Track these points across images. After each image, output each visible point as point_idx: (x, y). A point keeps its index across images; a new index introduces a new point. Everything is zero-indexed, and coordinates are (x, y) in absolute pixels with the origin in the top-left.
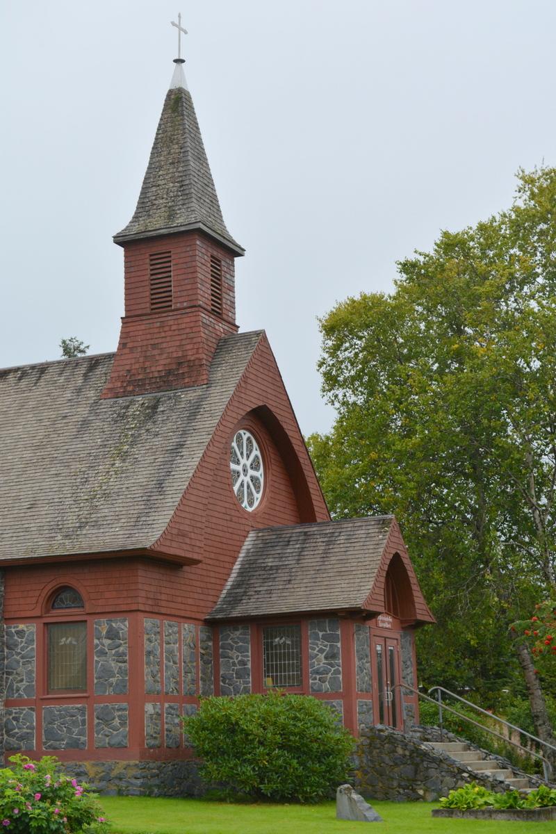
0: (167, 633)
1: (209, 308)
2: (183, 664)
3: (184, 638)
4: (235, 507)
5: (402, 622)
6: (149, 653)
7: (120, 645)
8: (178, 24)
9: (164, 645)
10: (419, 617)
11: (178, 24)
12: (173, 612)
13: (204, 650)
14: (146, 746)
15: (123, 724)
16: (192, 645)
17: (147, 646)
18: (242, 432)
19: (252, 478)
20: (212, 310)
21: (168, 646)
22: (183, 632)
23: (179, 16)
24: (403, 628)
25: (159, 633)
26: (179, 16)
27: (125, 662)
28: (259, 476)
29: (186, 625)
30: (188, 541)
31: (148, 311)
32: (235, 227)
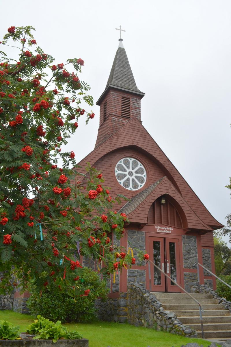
1: (120, 116)
4: (118, 188)
5: (184, 230)
8: (119, 28)
10: (189, 227)
11: (119, 28)
18: (128, 158)
20: (122, 116)
23: (120, 26)
24: (186, 234)
26: (120, 26)
28: (144, 177)
32: (140, 86)
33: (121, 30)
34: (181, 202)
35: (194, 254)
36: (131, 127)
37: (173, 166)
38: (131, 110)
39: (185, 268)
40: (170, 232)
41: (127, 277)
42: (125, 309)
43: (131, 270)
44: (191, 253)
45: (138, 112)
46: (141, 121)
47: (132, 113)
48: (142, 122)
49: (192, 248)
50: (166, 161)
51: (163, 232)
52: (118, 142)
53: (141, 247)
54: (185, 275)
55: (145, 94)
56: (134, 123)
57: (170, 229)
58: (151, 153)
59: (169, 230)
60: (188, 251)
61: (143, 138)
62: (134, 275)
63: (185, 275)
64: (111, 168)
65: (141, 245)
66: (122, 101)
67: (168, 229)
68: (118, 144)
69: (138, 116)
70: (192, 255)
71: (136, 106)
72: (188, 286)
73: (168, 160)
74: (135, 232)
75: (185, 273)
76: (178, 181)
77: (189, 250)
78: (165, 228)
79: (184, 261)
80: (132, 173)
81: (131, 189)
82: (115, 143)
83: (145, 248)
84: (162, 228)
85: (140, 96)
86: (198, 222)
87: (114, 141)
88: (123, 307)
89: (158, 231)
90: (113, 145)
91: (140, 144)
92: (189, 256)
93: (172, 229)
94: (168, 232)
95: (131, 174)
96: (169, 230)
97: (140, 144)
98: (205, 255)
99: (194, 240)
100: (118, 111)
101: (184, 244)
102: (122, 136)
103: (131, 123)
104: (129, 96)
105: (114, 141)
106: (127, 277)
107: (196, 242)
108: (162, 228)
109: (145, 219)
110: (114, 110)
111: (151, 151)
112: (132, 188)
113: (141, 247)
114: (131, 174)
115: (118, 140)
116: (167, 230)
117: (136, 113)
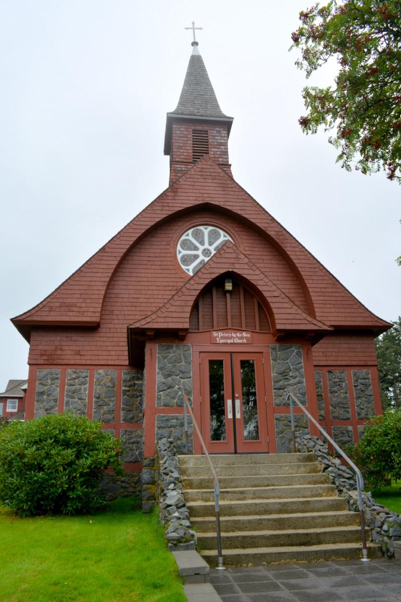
0: (69, 378)
1: (191, 161)
2: (94, 399)
3: (97, 380)
5: (274, 335)
6: (42, 393)
8: (192, 27)
9: (66, 386)
10: (279, 327)
11: (192, 27)
12: (84, 362)
13: (129, 387)
16: (110, 384)
18: (201, 228)
21: (70, 387)
22: (96, 376)
26: (193, 23)
29: (101, 371)
30: (76, 309)
32: (226, 109)
33: (194, 29)
34: (260, 283)
35: (297, 379)
36: (200, 173)
37: (282, 229)
38: (209, 149)
39: (279, 405)
40: (245, 341)
41: (156, 429)
42: (150, 488)
43: (163, 417)
44: (291, 377)
45: (224, 150)
46: (230, 163)
47: (212, 153)
48: (230, 165)
49: (292, 367)
50: (268, 221)
51: (229, 341)
52: (177, 201)
53: (183, 373)
54: (277, 419)
55: (233, 118)
56: (204, 166)
57: (244, 334)
58: (239, 212)
59: (242, 338)
60: (284, 374)
61: (223, 189)
62: (170, 424)
63: (277, 419)
64: (168, 247)
65: (183, 369)
66: (194, 137)
67: (239, 335)
68: (176, 205)
69: (224, 156)
70: (292, 381)
71: (219, 141)
72: (284, 440)
73: (273, 219)
74: (170, 347)
75: (277, 415)
76: (293, 253)
77: (284, 372)
78: (234, 335)
79: (275, 393)
80: (209, 252)
82: (170, 205)
83: (191, 375)
84: (227, 335)
85: (226, 124)
86: (298, 317)
87: (168, 201)
88: (148, 484)
89: (218, 342)
90: (167, 208)
91: (217, 199)
92: (286, 383)
93: (249, 335)
94: (240, 341)
96: (242, 338)
97: (217, 199)
98: (360, 381)
99: (295, 351)
100: (185, 154)
101: (275, 360)
102: (182, 190)
103: (200, 166)
104: (205, 128)
105: (168, 201)
106: (156, 429)
107: (300, 356)
108: (227, 335)
109: (183, 320)
110: (178, 153)
111: (238, 208)
113: (183, 373)
114: (207, 253)
115: (176, 198)
116: (237, 337)
117: (219, 153)
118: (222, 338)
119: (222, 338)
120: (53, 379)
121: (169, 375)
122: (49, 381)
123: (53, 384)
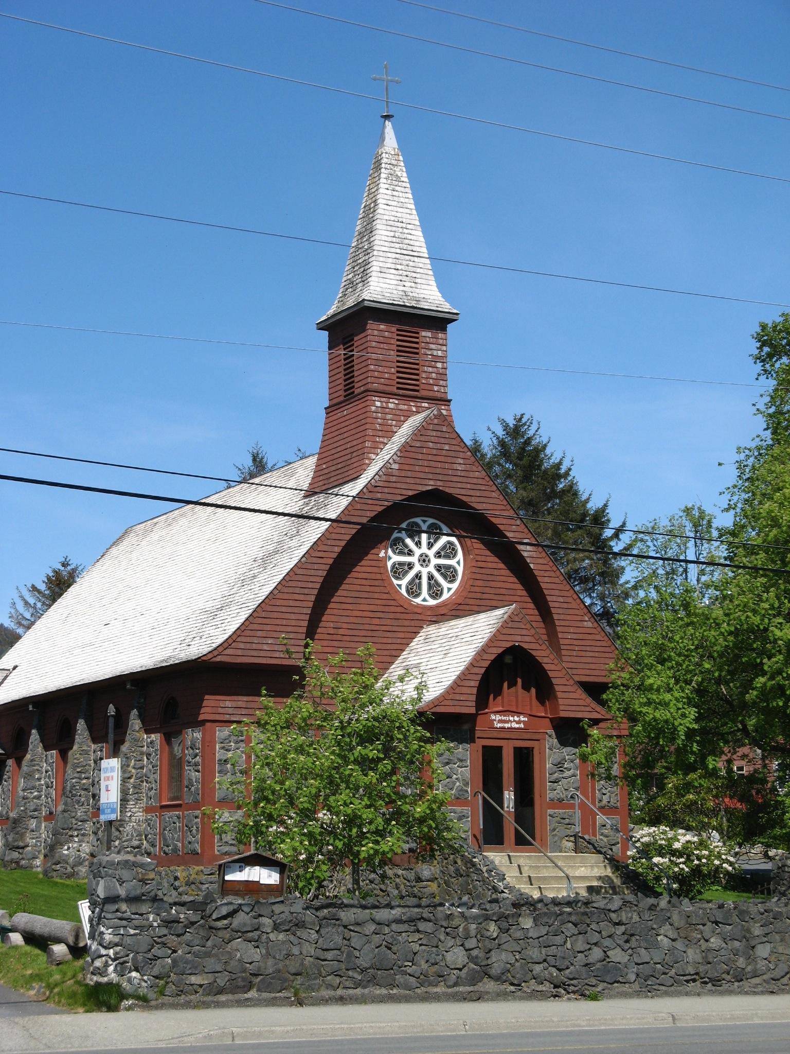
1: (394, 390)
7: (196, 755)
14: (216, 852)
15: (197, 831)
17: (219, 754)
19: (439, 568)
20: (398, 388)
25: (242, 741)
27: (198, 771)
31: (342, 398)
34: (545, 660)
35: (572, 771)
38: (421, 369)
39: (552, 800)
40: (522, 726)
42: (429, 886)
44: (565, 768)
45: (441, 371)
47: (424, 375)
48: (450, 401)
49: (567, 757)
51: (507, 725)
53: (461, 761)
54: (550, 815)
57: (522, 718)
59: (519, 722)
60: (559, 765)
63: (550, 815)
65: (460, 756)
67: (516, 718)
69: (441, 383)
70: (567, 773)
71: (435, 353)
72: (556, 838)
75: (550, 811)
76: (542, 573)
77: (559, 763)
78: (511, 719)
79: (550, 786)
80: (427, 560)
81: (424, 600)
83: (468, 763)
84: (504, 718)
86: (581, 702)
89: (495, 726)
92: (561, 776)
93: (526, 719)
94: (517, 726)
95: (424, 560)
96: (519, 722)
99: (572, 738)
100: (387, 376)
101: (550, 749)
108: (504, 718)
110: (376, 374)
112: (428, 598)
113: (461, 761)
114: (424, 561)
116: (514, 721)
117: (434, 375)
118: (500, 721)
119: (500, 721)
120: (237, 742)
121: (447, 763)
122: (232, 744)
123: (238, 749)
